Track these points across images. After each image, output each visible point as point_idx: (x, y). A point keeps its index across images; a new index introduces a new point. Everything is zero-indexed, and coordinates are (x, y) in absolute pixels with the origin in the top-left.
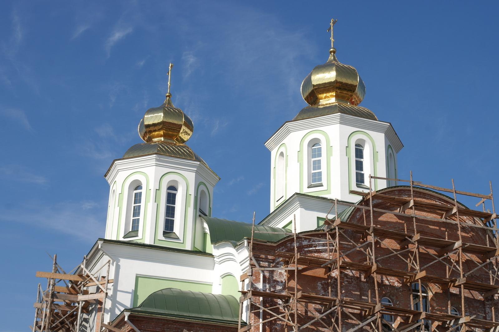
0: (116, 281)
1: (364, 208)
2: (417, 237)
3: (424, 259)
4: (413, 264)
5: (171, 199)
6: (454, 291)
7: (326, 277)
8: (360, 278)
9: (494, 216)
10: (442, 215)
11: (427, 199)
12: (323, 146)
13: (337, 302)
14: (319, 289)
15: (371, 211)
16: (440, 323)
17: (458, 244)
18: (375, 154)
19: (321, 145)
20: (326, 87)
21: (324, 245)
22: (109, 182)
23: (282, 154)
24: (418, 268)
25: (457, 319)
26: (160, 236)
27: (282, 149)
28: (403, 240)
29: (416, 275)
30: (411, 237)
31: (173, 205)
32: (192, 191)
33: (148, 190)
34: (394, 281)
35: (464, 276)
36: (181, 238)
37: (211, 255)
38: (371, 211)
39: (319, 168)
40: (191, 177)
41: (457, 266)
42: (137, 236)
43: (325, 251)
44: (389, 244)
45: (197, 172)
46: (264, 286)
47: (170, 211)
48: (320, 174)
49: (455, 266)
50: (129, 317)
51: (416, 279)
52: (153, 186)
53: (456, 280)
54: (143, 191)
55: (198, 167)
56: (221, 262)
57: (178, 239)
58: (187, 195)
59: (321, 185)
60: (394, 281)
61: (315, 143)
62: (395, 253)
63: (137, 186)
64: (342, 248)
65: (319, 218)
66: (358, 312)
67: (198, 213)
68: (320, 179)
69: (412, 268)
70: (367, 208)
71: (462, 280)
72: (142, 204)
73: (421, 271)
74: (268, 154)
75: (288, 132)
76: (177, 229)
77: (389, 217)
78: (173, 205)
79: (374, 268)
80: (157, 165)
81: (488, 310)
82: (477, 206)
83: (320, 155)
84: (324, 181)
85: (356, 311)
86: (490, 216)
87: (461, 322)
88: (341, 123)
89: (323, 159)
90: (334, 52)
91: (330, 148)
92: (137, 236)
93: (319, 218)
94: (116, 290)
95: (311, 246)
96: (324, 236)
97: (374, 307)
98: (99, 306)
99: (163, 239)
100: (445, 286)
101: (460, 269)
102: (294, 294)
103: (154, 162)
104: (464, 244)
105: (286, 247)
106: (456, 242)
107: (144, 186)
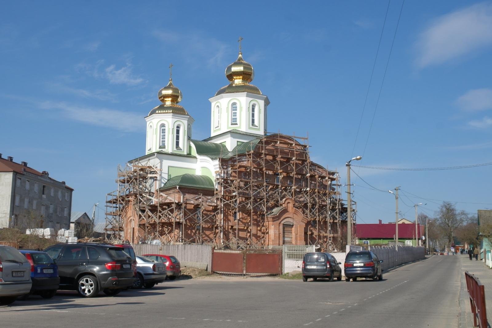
0: (161, 170)
1: (260, 145)
2: (280, 156)
3: (282, 163)
4: (277, 166)
5: (178, 132)
6: (291, 175)
7: (245, 171)
8: (258, 171)
9: (308, 146)
10: (289, 145)
11: (284, 139)
12: (238, 106)
13: (251, 182)
14: (243, 175)
15: (264, 147)
16: (284, 188)
17: (294, 158)
18: (260, 110)
19: (236, 105)
20: (237, 74)
21: (245, 159)
22: (147, 120)
23: (218, 106)
24: (279, 168)
25: (291, 187)
26: (175, 149)
27: (218, 104)
28: (274, 157)
29: (278, 171)
30: (277, 156)
31: (178, 135)
32: (186, 129)
33: (169, 129)
34: (271, 173)
35: (295, 171)
36: (183, 149)
37: (195, 157)
38: (264, 147)
39: (236, 116)
40: (186, 122)
41: (293, 167)
42: (165, 148)
43: (245, 161)
44: (270, 158)
45: (188, 120)
46: (224, 175)
47: (178, 138)
48: (236, 119)
49: (292, 167)
50: (179, 188)
51: (278, 172)
52: (171, 127)
53: (292, 172)
54: (166, 128)
55: (189, 118)
56: (201, 162)
57: (181, 150)
58: (185, 131)
59: (236, 124)
60: (271, 173)
61: (234, 104)
62: (271, 163)
63: (163, 125)
64: (254, 162)
65: (238, 142)
66: (256, 184)
67: (188, 138)
68: (236, 121)
69: (276, 168)
70: (262, 145)
71: (295, 173)
72: (166, 134)
73: (280, 169)
74: (210, 104)
75: (222, 98)
76: (181, 145)
77: (269, 147)
78: (178, 135)
79: (264, 169)
80: (172, 118)
81: (302, 182)
82: (302, 142)
83: (236, 110)
84: (238, 122)
85: (255, 184)
86: (306, 146)
87: (293, 188)
88: (246, 96)
89: (238, 112)
90: (241, 54)
91: (241, 108)
92: (165, 148)
93: (238, 142)
94: (161, 173)
95: (240, 159)
96: (245, 155)
97: (263, 184)
98: (155, 178)
99: (176, 150)
100: (288, 173)
101: (294, 168)
102: (236, 180)
103: (171, 116)
104: (296, 158)
105: (231, 160)
106: (293, 158)
107: (166, 126)
